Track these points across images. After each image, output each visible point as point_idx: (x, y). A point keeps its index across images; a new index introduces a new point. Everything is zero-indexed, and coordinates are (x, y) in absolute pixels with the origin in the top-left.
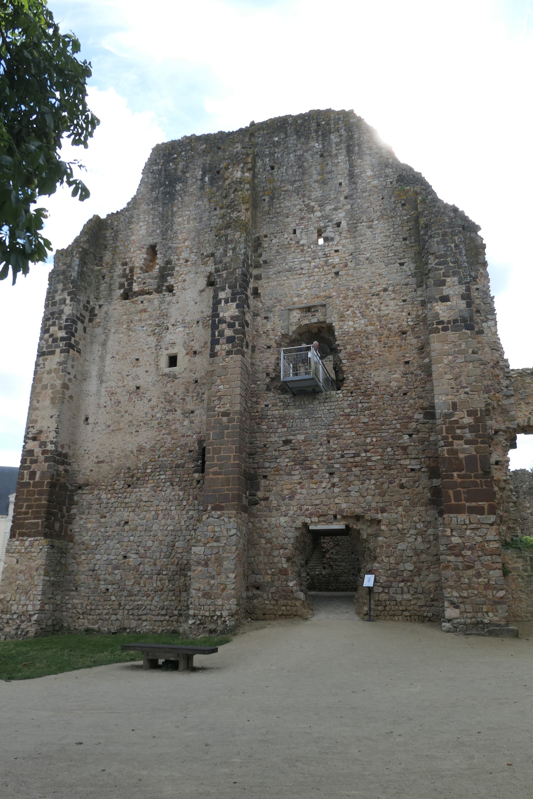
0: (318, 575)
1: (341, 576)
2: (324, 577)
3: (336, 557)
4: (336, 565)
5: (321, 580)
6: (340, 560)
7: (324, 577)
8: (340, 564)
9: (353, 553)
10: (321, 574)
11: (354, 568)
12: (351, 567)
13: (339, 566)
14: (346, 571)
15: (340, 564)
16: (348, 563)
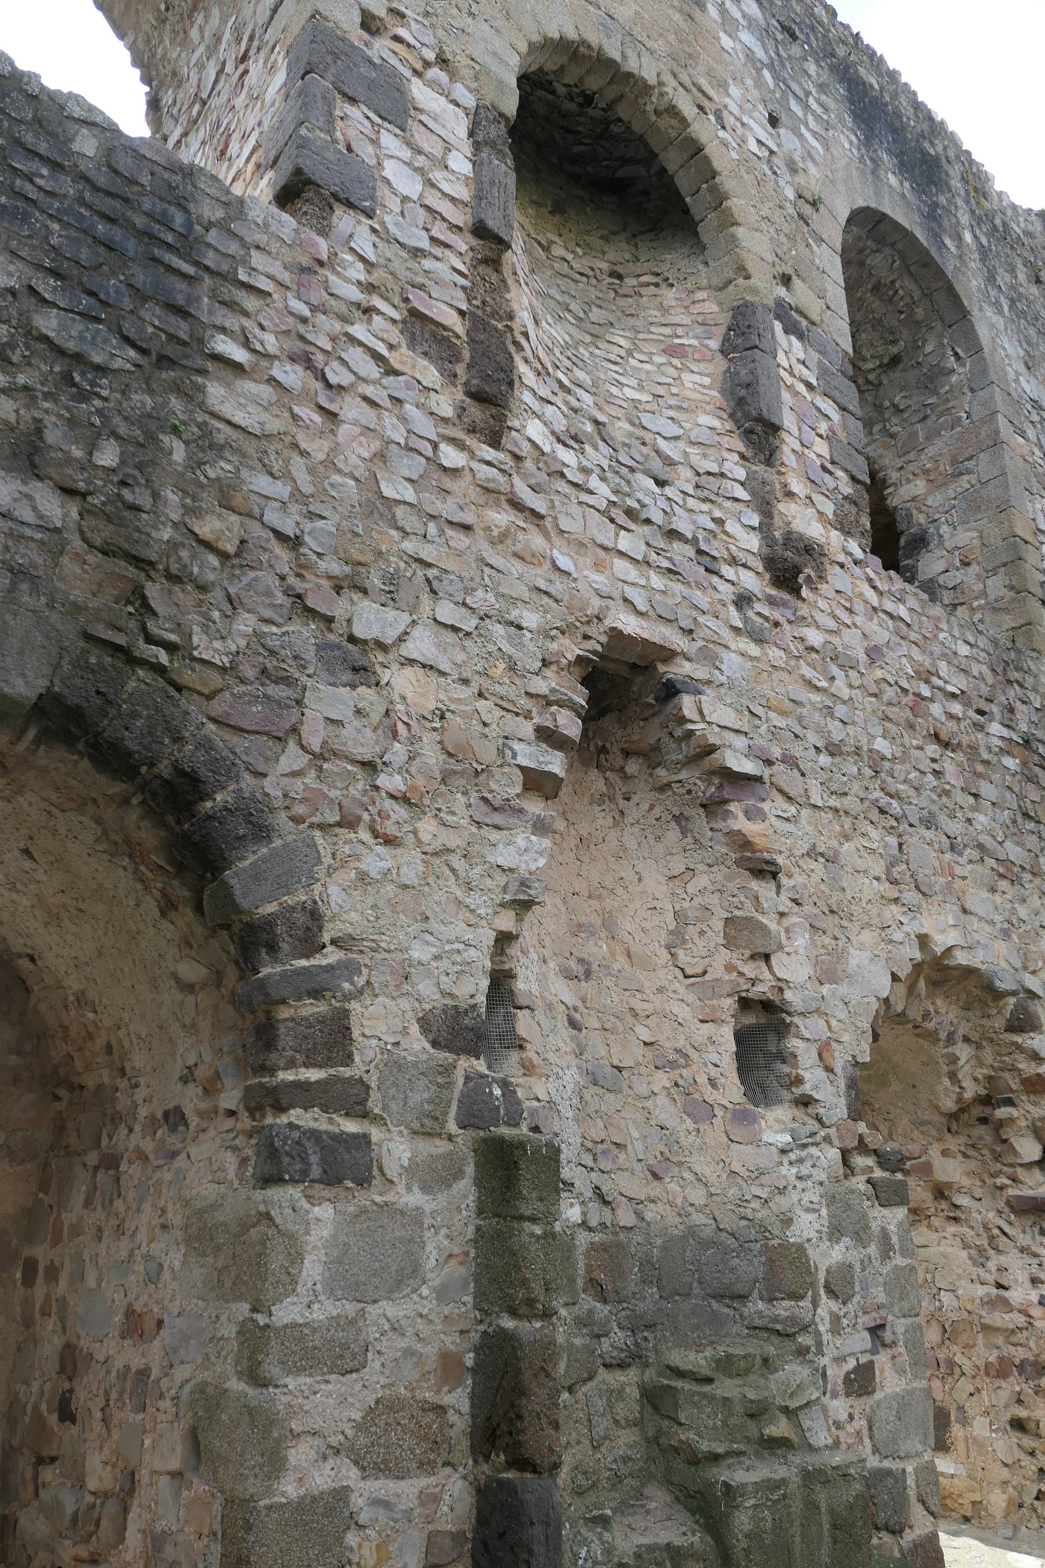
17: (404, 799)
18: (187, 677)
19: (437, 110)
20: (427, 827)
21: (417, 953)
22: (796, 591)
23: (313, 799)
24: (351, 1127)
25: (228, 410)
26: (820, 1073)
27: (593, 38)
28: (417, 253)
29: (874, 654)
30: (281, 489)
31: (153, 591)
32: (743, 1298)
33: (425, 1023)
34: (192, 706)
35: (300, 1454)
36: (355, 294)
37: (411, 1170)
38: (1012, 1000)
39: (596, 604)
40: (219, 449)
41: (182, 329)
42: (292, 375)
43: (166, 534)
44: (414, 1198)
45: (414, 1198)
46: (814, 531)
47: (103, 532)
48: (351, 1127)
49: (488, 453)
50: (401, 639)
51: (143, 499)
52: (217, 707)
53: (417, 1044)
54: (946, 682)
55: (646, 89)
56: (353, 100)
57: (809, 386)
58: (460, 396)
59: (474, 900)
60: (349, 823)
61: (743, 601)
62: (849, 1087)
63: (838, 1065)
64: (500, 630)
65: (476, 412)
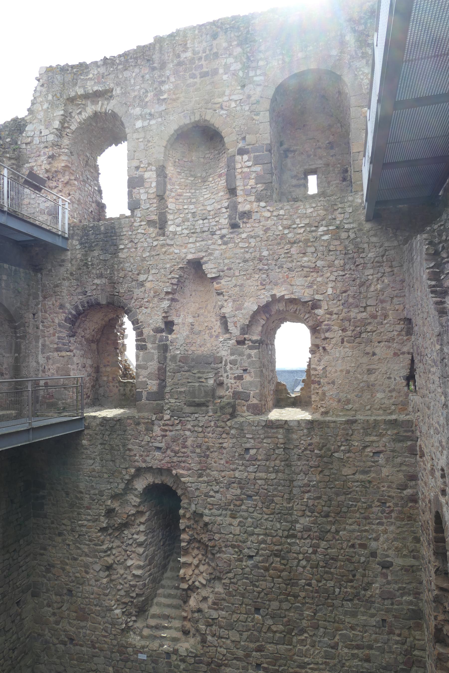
0: (168, 654)
1: (226, 665)
2: (183, 660)
3: (215, 614)
4: (214, 635)
5: (178, 667)
6: (223, 622)
7: (183, 660)
8: (223, 632)
9: (257, 610)
10: (176, 652)
11: (259, 649)
12: (252, 645)
13: (220, 637)
14: (240, 653)
15: (223, 632)
16: (245, 635)
17: (147, 302)
18: (120, 295)
19: (149, 176)
20: (151, 305)
21: (151, 322)
22: (239, 227)
23: (136, 305)
24: (144, 343)
25: (123, 256)
26: (234, 328)
27: (182, 124)
28: (148, 209)
29: (266, 230)
30: (129, 264)
31: (115, 286)
32: (211, 364)
33: (153, 330)
34: (122, 299)
35: (141, 377)
36: (139, 224)
37: (152, 348)
38: (311, 302)
39: (183, 256)
40: (121, 263)
41: (116, 247)
42: (130, 245)
43: (116, 278)
44: (153, 351)
45: (153, 351)
46: (247, 207)
47: (110, 281)
48: (144, 343)
49: (162, 238)
50: (147, 278)
51: (113, 275)
52: (124, 298)
53: (152, 333)
54: (298, 224)
55: (199, 121)
56: (135, 188)
57: (249, 167)
58: (158, 230)
59: (158, 313)
60: (141, 307)
61: (222, 237)
62: (241, 329)
63: (238, 326)
64: (163, 270)
65: (161, 232)
